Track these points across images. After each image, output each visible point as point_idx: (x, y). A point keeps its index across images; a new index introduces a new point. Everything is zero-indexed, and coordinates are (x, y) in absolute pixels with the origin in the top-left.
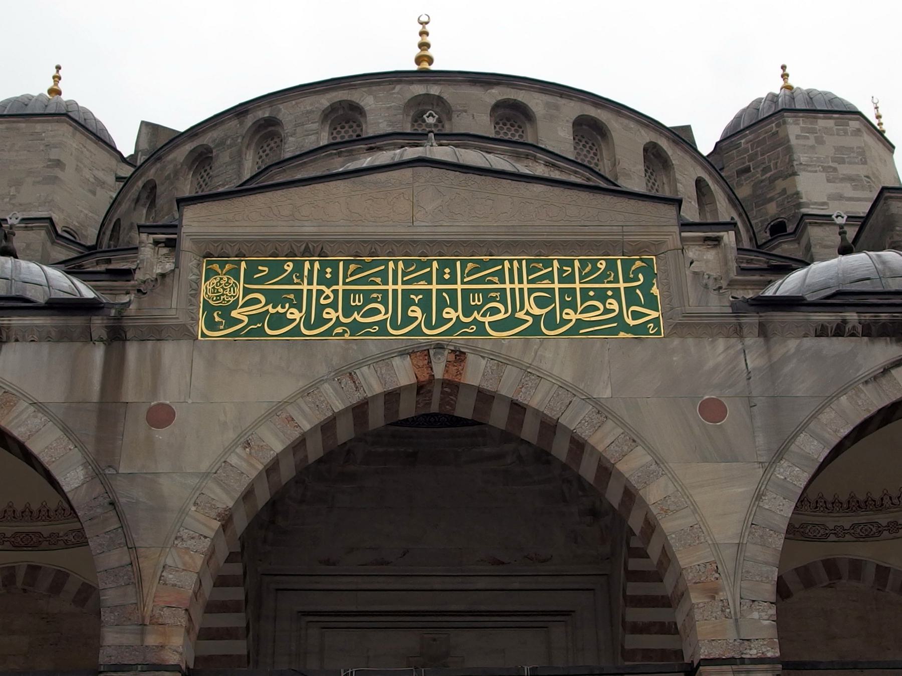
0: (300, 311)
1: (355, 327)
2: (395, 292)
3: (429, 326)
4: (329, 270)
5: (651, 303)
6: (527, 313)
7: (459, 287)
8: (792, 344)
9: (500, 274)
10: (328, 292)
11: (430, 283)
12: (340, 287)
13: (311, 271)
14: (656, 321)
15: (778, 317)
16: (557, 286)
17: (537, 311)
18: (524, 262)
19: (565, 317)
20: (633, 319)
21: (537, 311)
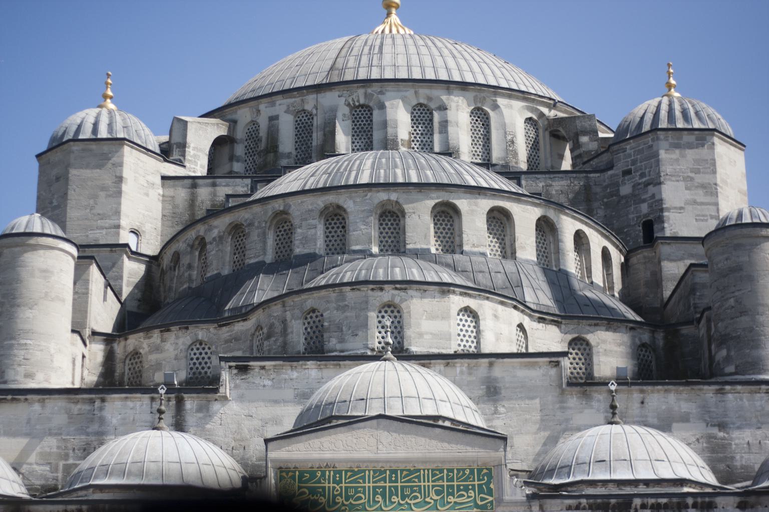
0: (325, 498)
2: (369, 487)
3: (386, 506)
4: (338, 476)
5: (490, 493)
6: (431, 499)
7: (399, 484)
9: (418, 477)
10: (338, 487)
11: (386, 482)
12: (343, 485)
13: (329, 476)
14: (491, 502)
16: (445, 483)
17: (436, 498)
18: (430, 471)
19: (449, 500)
20: (481, 501)
21: (436, 498)
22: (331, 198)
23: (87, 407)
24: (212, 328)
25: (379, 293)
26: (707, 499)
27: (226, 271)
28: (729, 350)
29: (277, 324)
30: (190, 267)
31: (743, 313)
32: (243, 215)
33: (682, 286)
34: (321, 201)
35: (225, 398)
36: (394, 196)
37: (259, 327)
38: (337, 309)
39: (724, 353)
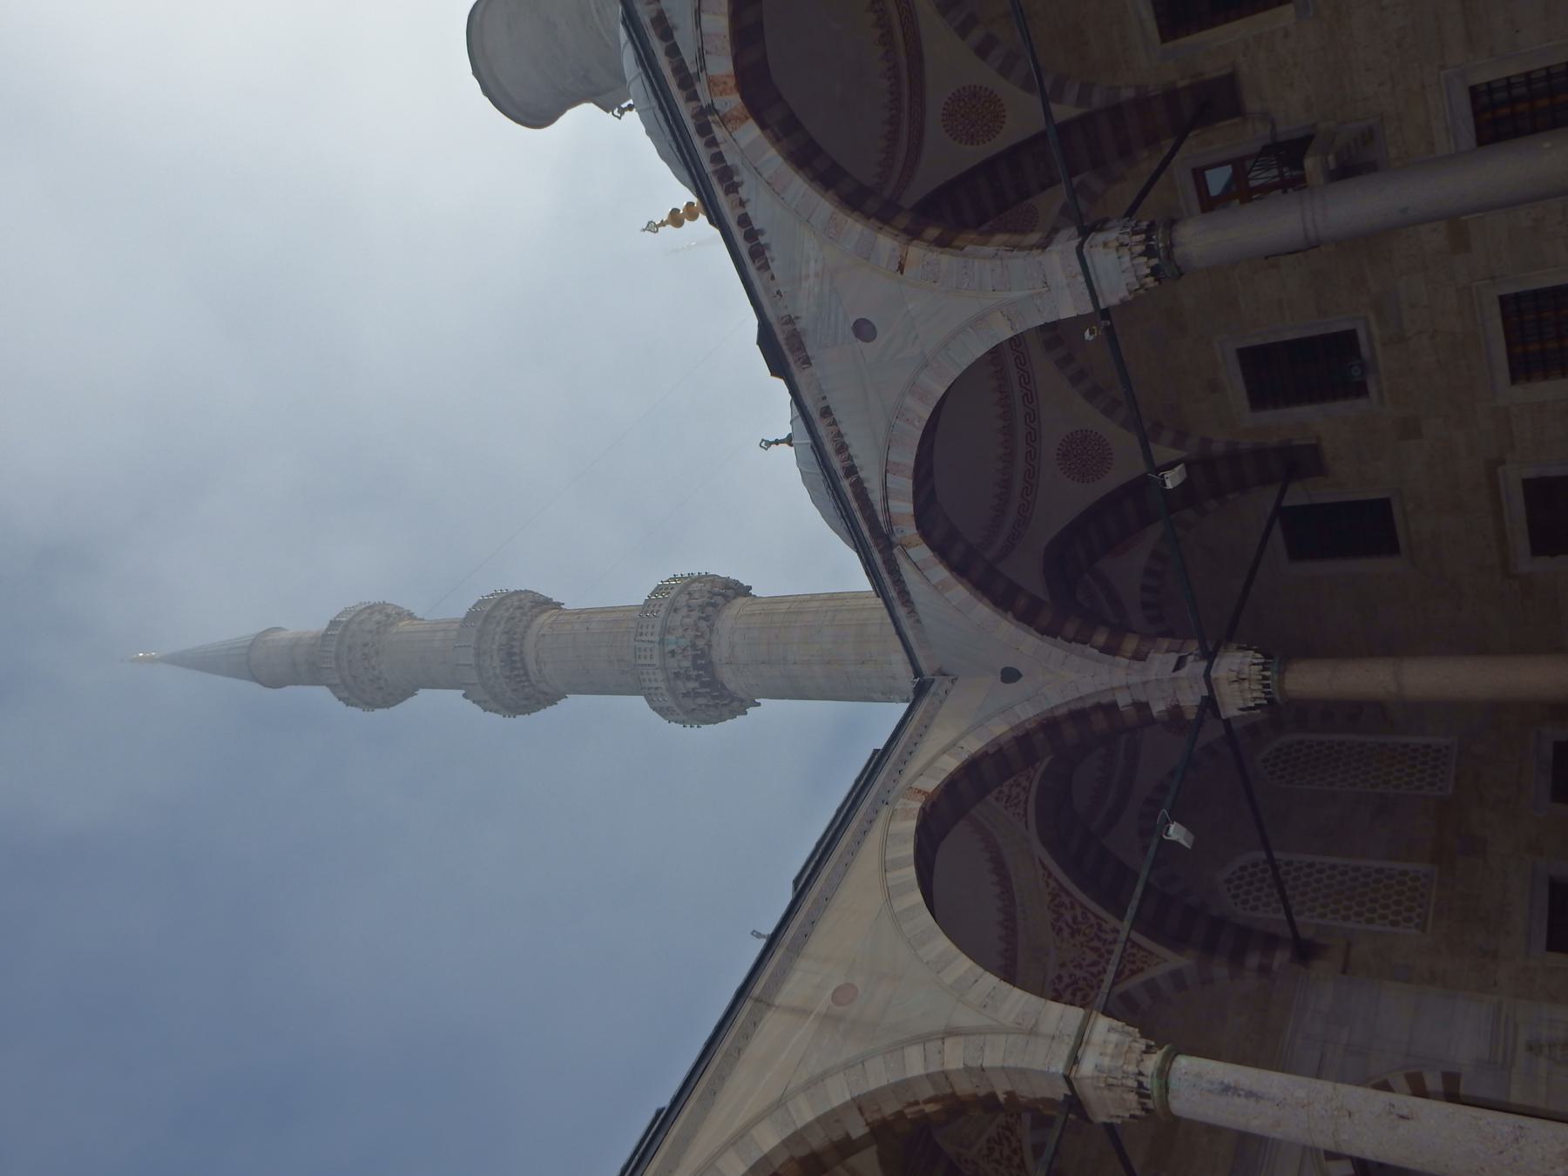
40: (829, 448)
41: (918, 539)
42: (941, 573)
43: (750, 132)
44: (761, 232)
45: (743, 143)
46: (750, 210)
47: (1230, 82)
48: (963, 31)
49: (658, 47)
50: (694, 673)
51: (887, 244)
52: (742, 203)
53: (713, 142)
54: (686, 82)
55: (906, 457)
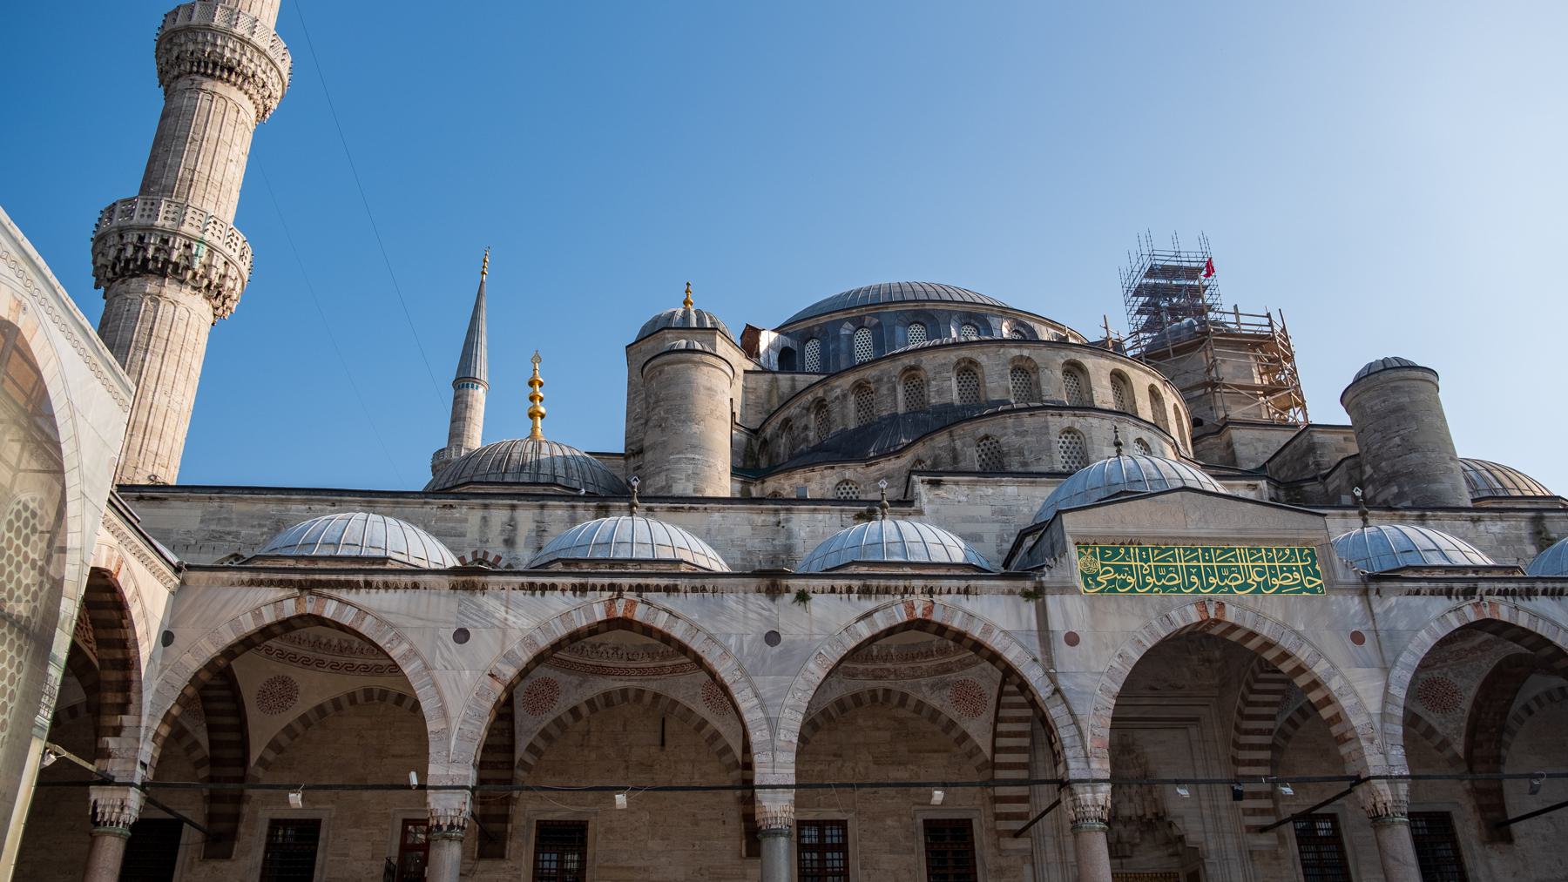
1: (1165, 588)
5: (1317, 574)
8: (1393, 600)
15: (1386, 585)
22: (965, 353)
23: (772, 519)
24: (860, 468)
25: (1057, 419)
26: (1558, 585)
27: (852, 426)
28: (1400, 486)
29: (944, 454)
30: (806, 428)
31: (1411, 451)
32: (870, 373)
33: (1287, 451)
34: (953, 356)
35: (920, 512)
36: (1026, 353)
37: (920, 461)
38: (1016, 434)
39: (1395, 489)
40: (391, 578)
41: (301, 611)
42: (269, 617)
43: (600, 614)
44: (543, 594)
45: (595, 606)
46: (558, 593)
47: (502, 856)
48: (590, 703)
49: (663, 582)
50: (161, 257)
51: (510, 672)
52: (563, 590)
53: (603, 588)
54: (640, 589)
55: (366, 628)
